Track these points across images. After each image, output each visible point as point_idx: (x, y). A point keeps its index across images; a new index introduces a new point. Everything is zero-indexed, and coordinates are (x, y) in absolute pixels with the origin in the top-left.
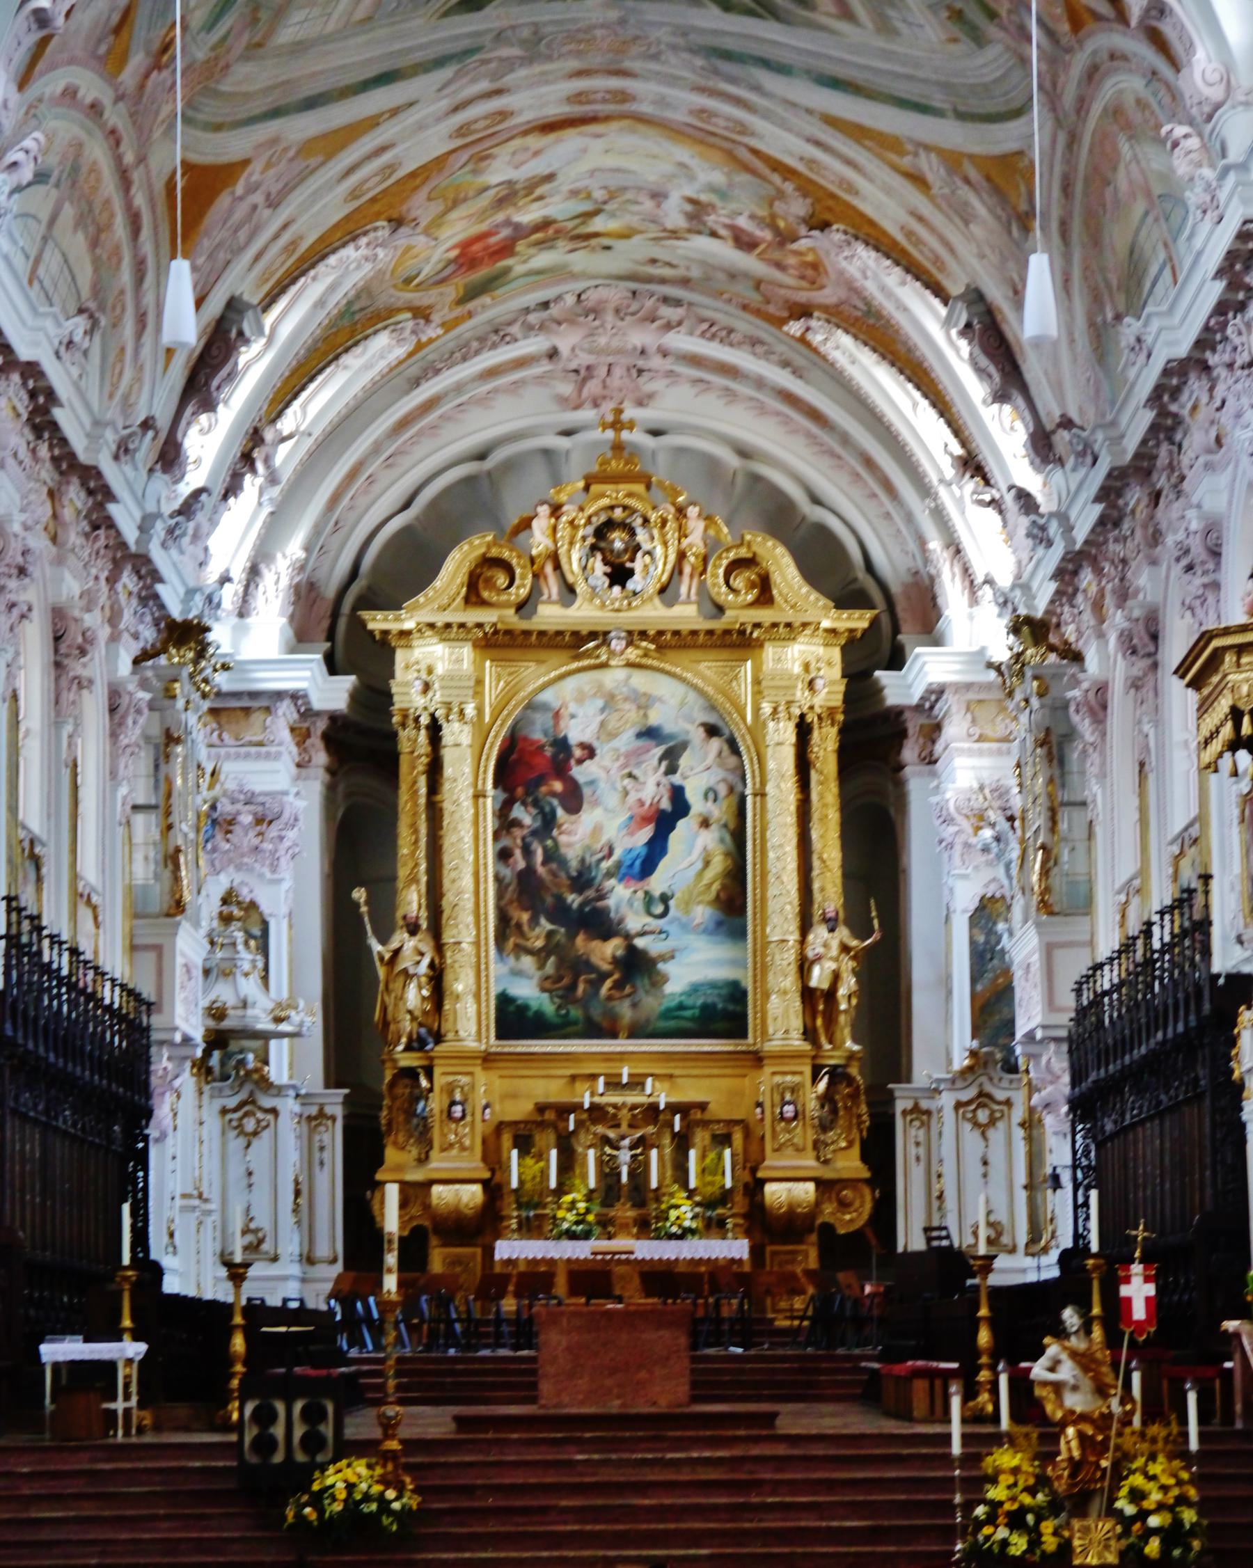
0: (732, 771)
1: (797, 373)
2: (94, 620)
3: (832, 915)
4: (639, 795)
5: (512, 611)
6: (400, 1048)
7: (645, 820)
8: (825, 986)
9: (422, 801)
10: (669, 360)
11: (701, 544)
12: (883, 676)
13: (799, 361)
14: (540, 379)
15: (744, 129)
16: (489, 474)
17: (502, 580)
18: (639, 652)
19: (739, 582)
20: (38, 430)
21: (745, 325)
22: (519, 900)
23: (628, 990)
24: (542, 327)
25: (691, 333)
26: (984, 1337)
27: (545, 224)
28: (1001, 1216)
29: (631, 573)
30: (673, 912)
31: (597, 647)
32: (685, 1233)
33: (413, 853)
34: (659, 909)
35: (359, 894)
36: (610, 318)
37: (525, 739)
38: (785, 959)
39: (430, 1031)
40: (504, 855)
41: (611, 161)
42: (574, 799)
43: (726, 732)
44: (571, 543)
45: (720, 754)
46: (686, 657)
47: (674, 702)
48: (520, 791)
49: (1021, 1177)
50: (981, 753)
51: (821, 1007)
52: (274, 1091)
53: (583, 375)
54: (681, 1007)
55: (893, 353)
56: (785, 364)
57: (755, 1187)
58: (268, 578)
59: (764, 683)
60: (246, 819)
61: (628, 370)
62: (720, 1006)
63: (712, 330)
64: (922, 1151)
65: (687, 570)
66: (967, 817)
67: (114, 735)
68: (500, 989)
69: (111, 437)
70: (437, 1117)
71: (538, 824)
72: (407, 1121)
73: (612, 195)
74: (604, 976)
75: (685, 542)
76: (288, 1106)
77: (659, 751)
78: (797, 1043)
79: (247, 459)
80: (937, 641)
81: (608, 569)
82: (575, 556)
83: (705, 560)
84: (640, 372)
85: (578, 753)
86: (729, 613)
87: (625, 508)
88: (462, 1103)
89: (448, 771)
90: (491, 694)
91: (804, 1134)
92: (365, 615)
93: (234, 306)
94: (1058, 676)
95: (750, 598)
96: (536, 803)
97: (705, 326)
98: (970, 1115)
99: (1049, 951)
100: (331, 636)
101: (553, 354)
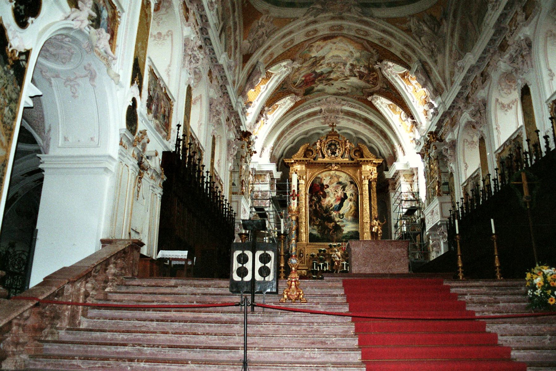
1: (368, 113)
7: (339, 200)
12: (385, 173)
14: (318, 119)
15: (367, 33)
17: (311, 154)
19: (357, 154)
24: (319, 105)
27: (322, 73)
34: (342, 217)
41: (336, 53)
42: (325, 195)
45: (353, 187)
46: (346, 168)
50: (407, 184)
58: (266, 149)
73: (336, 64)
77: (341, 187)
82: (325, 149)
85: (325, 187)
90: (309, 174)
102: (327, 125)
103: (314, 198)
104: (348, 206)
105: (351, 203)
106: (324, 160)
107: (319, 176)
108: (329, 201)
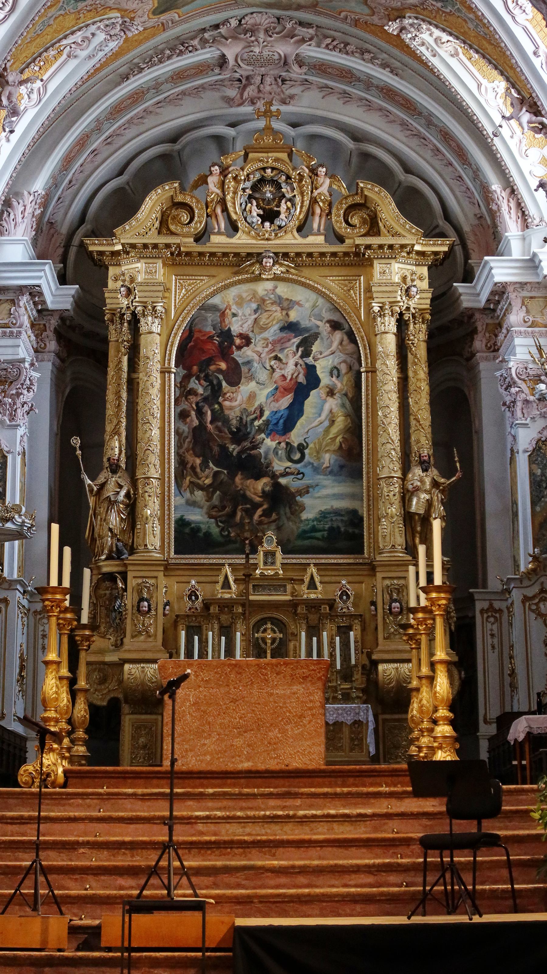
0: (350, 355)
3: (426, 458)
4: (283, 372)
5: (192, 240)
6: (103, 557)
7: (287, 390)
8: (422, 512)
9: (125, 375)
10: (304, 69)
11: (327, 194)
16: (179, 152)
18: (283, 269)
19: (355, 220)
22: (193, 449)
23: (274, 516)
25: (319, 46)
29: (278, 213)
30: (307, 458)
31: (252, 265)
33: (117, 415)
34: (297, 456)
35: (76, 441)
36: (261, 35)
37: (200, 331)
39: (125, 545)
40: (182, 416)
43: (346, 326)
44: (235, 193)
45: (341, 343)
47: (307, 305)
48: (195, 368)
51: (419, 529)
52: (6, 585)
54: (314, 529)
55: (464, 33)
56: (384, 66)
59: (374, 289)
61: (276, 80)
62: (342, 529)
64: (496, 641)
65: (318, 211)
66: (524, 380)
68: (179, 516)
70: (130, 612)
71: (209, 392)
72: (108, 616)
74: (256, 506)
75: (316, 193)
77: (296, 341)
81: (261, 212)
83: (330, 205)
84: (284, 81)
85: (238, 341)
86: (347, 241)
87: (273, 169)
88: (146, 600)
89: (143, 351)
92: (87, 241)
95: (363, 231)
96: (207, 378)
97: (329, 41)
98: (534, 607)
101: (222, 61)
103: (193, 384)
105: (332, 404)
106: (234, 240)
107: (216, 300)
108: (252, 396)
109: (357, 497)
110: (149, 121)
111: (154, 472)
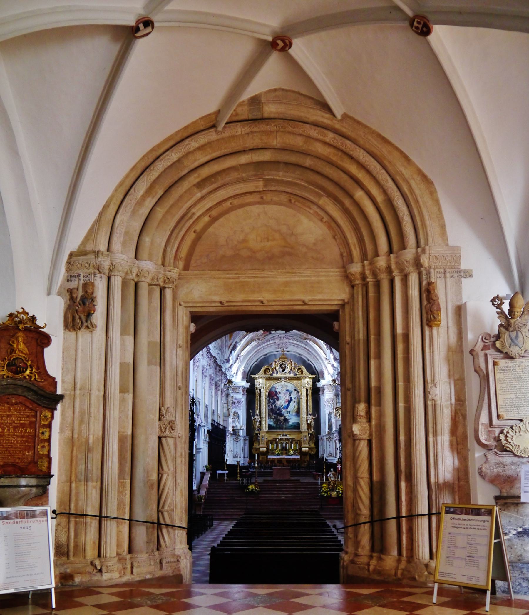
2: (220, 383)
13: (306, 344)
17: (269, 371)
19: (299, 371)
20: (214, 362)
21: (299, 339)
24: (274, 339)
26: (324, 470)
28: (332, 452)
32: (292, 455)
38: (305, 419)
40: (269, 406)
42: (278, 399)
49: (334, 448)
53: (279, 345)
56: (304, 344)
57: (301, 449)
58: (239, 371)
60: (237, 402)
63: (295, 340)
67: (222, 395)
69: (222, 361)
76: (242, 438)
78: (306, 430)
79: (237, 358)
80: (324, 379)
82: (278, 368)
89: (262, 395)
90: (267, 385)
91: (307, 442)
93: (236, 343)
94: (337, 387)
99: (336, 421)
100: (247, 378)
101: (275, 343)
102: (279, 350)
104: (293, 406)
107: (274, 386)
108: (281, 403)
109: (299, 420)
110: (262, 352)
111: (264, 417)
